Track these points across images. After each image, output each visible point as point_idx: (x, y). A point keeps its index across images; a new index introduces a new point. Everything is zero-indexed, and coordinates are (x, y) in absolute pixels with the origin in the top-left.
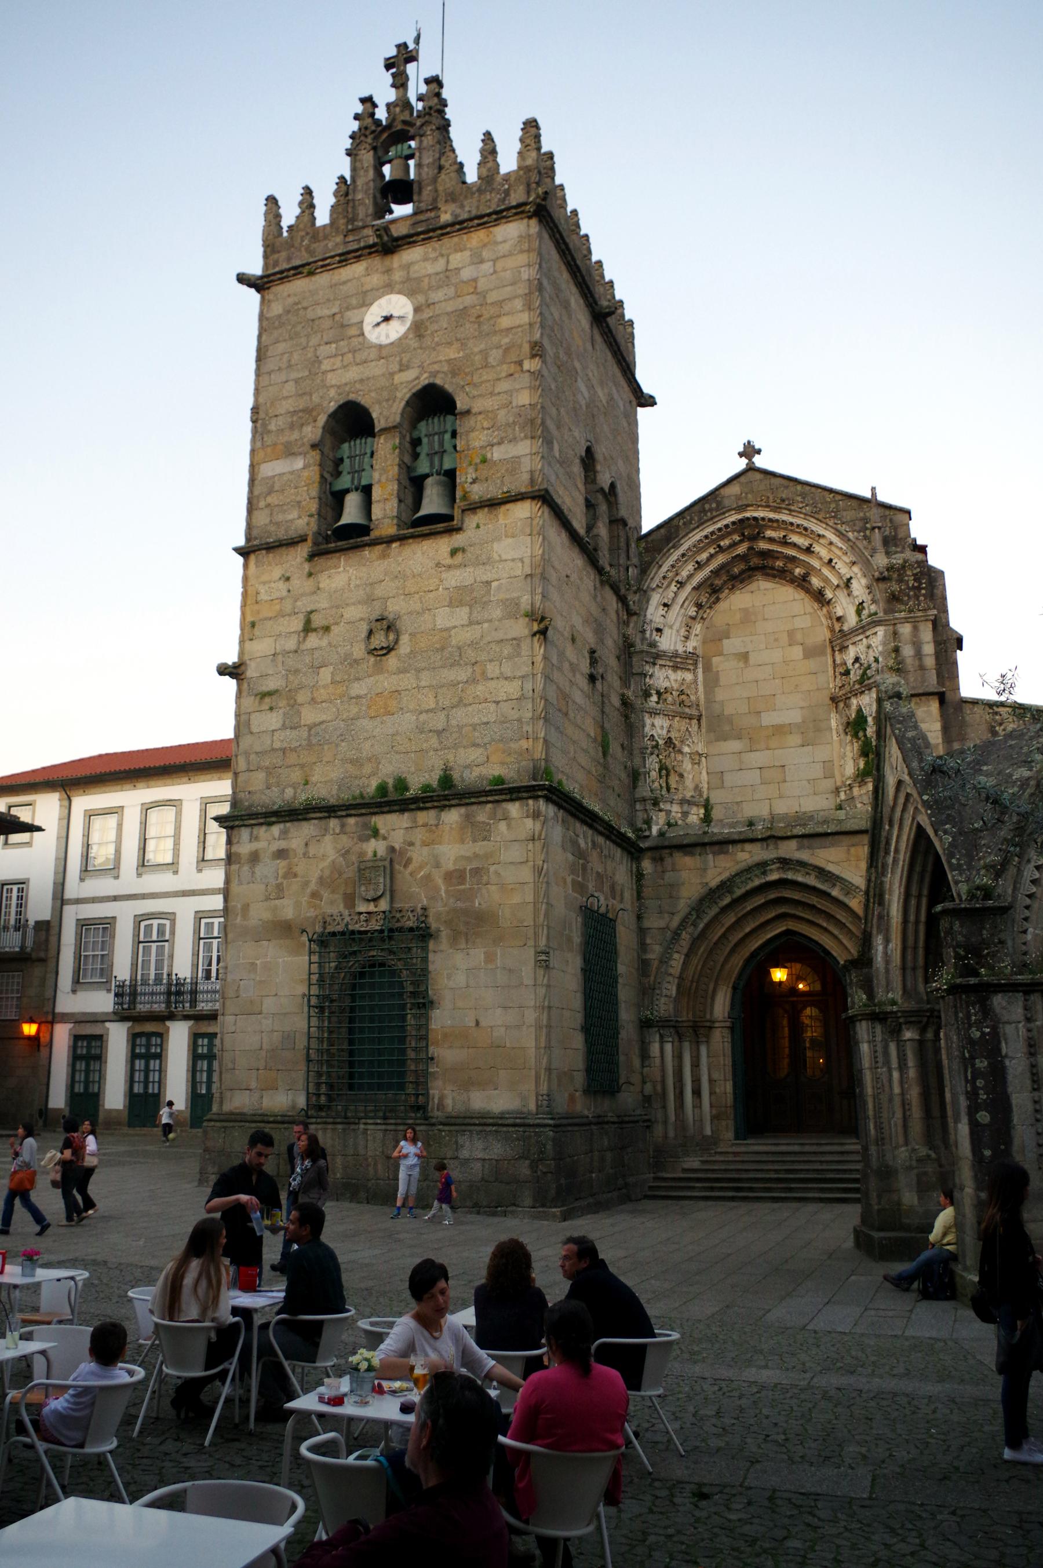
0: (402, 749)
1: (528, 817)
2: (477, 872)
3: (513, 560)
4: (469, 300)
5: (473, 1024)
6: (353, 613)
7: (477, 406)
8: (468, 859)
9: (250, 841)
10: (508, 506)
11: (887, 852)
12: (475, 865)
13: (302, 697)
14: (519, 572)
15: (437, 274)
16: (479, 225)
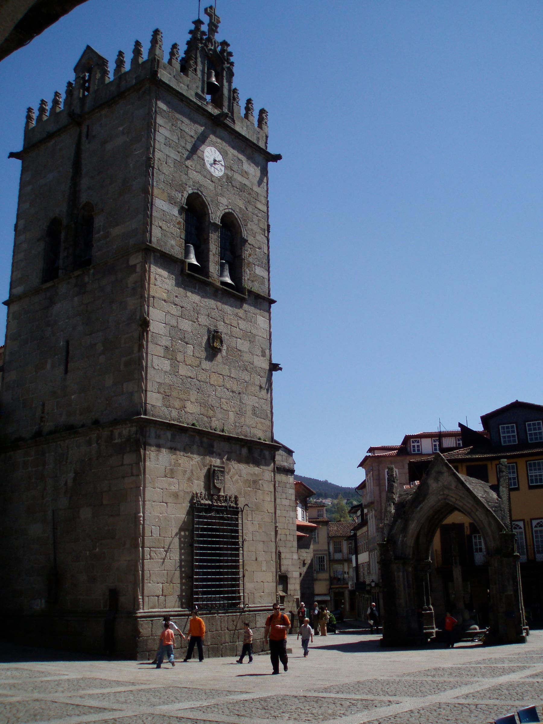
0: (223, 406)
1: (271, 459)
2: (255, 482)
3: (263, 329)
4: (245, 181)
5: (254, 559)
6: (203, 320)
7: (251, 240)
8: (251, 474)
9: (156, 438)
10: (261, 300)
11: (417, 507)
12: (255, 478)
13: (180, 357)
14: (266, 337)
15: (234, 156)
16: (251, 147)
